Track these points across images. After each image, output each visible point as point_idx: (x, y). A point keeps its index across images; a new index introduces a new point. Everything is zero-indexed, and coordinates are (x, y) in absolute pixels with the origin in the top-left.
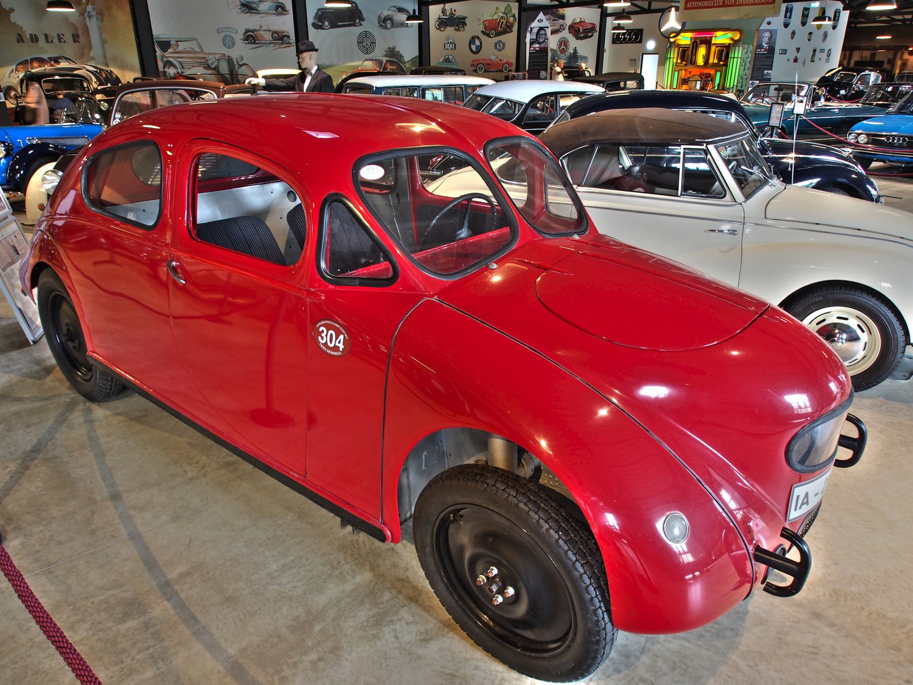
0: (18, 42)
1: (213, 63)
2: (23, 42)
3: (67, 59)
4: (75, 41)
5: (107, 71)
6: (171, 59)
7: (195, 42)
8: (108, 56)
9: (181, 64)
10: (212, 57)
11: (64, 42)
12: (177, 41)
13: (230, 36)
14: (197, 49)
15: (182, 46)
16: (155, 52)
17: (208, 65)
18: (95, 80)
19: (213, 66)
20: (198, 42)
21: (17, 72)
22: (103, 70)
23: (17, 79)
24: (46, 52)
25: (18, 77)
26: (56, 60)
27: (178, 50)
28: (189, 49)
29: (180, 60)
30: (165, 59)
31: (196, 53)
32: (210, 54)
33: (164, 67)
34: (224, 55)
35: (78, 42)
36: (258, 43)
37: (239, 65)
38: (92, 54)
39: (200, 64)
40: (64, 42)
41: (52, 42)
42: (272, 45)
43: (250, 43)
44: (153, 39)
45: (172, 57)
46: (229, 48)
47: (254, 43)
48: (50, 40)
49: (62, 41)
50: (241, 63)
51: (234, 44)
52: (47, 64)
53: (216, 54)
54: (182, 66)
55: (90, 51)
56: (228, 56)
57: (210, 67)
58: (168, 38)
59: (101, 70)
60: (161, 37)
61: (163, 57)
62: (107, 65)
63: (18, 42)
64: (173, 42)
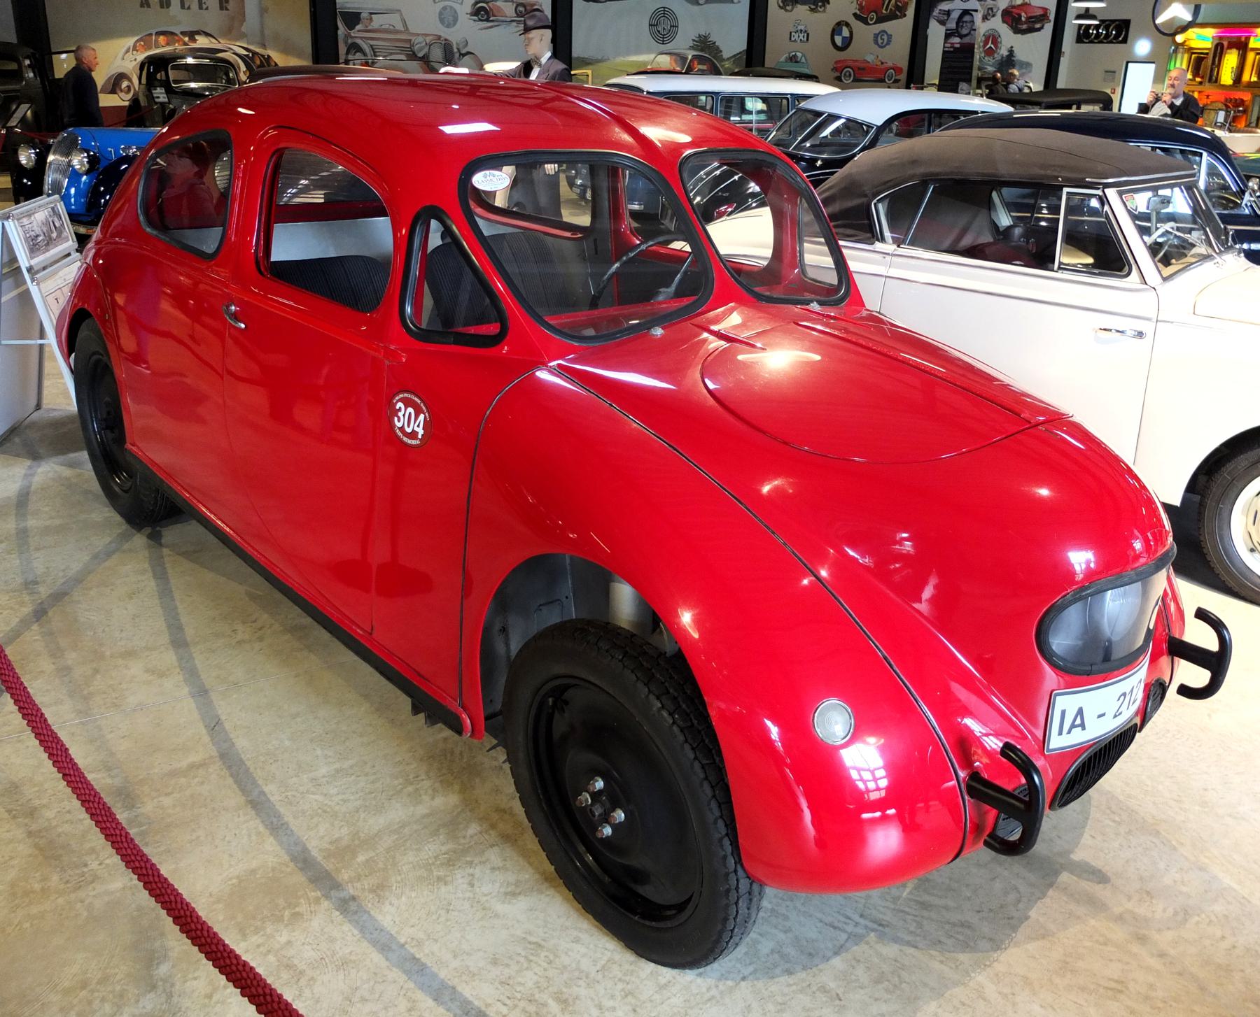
0: (142, 6)
1: (421, 49)
2: (149, 6)
3: (207, 35)
4: (221, 8)
5: (263, 56)
6: (359, 41)
7: (397, 16)
8: (266, 32)
9: (373, 49)
10: (420, 39)
11: (207, 9)
12: (371, 13)
13: (451, 7)
14: (400, 27)
15: (377, 21)
16: (337, 28)
17: (414, 53)
18: (245, 69)
19: (420, 55)
20: (401, 15)
21: (135, 52)
22: (257, 53)
23: (134, 63)
24: (179, 23)
25: (135, 60)
26: (192, 35)
27: (370, 28)
28: (387, 27)
29: (372, 43)
30: (350, 41)
31: (398, 32)
32: (418, 35)
33: (348, 53)
34: (439, 37)
35: (227, 9)
36: (493, 21)
37: (461, 54)
38: (243, 29)
39: (402, 49)
40: (207, 9)
41: (189, 8)
42: (514, 24)
43: (480, 20)
44: (336, 9)
45: (361, 38)
46: (448, 26)
47: (487, 20)
48: (186, 6)
49: (204, 6)
50: (463, 51)
51: (456, 20)
52: (178, 41)
53: (427, 35)
54: (374, 52)
55: (242, 25)
56: (446, 40)
57: (416, 56)
58: (359, 8)
59: (254, 53)
60: (348, 5)
61: (348, 36)
62: (264, 46)
63: (142, 6)
64: (363, 15)
